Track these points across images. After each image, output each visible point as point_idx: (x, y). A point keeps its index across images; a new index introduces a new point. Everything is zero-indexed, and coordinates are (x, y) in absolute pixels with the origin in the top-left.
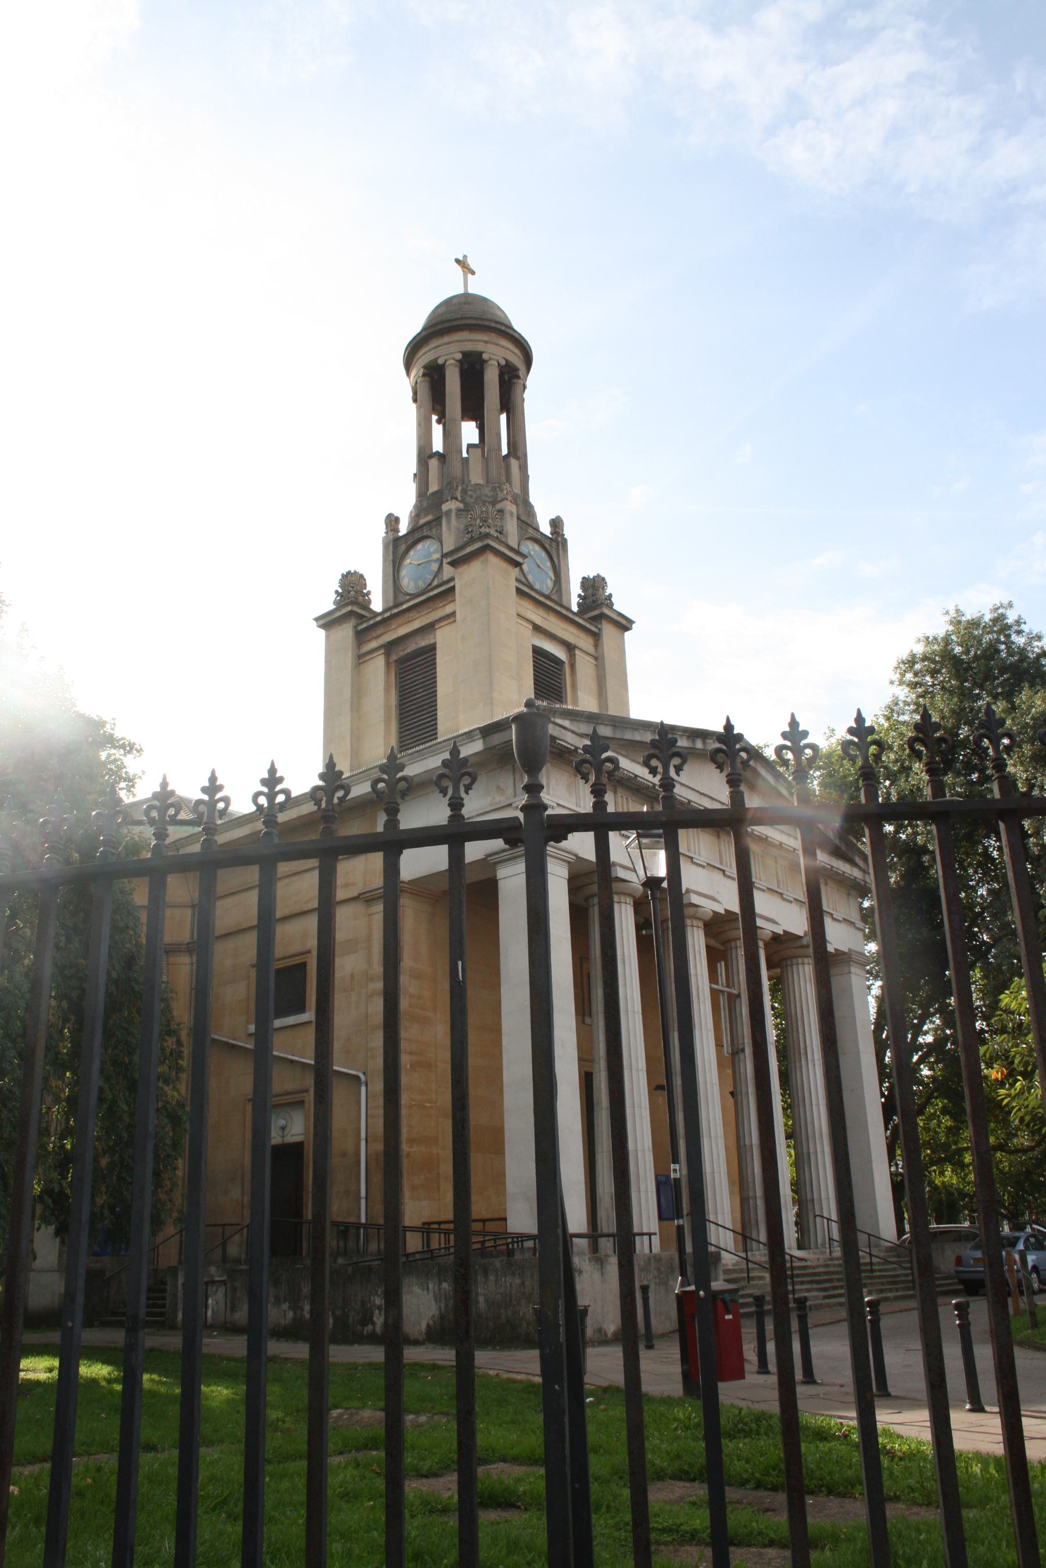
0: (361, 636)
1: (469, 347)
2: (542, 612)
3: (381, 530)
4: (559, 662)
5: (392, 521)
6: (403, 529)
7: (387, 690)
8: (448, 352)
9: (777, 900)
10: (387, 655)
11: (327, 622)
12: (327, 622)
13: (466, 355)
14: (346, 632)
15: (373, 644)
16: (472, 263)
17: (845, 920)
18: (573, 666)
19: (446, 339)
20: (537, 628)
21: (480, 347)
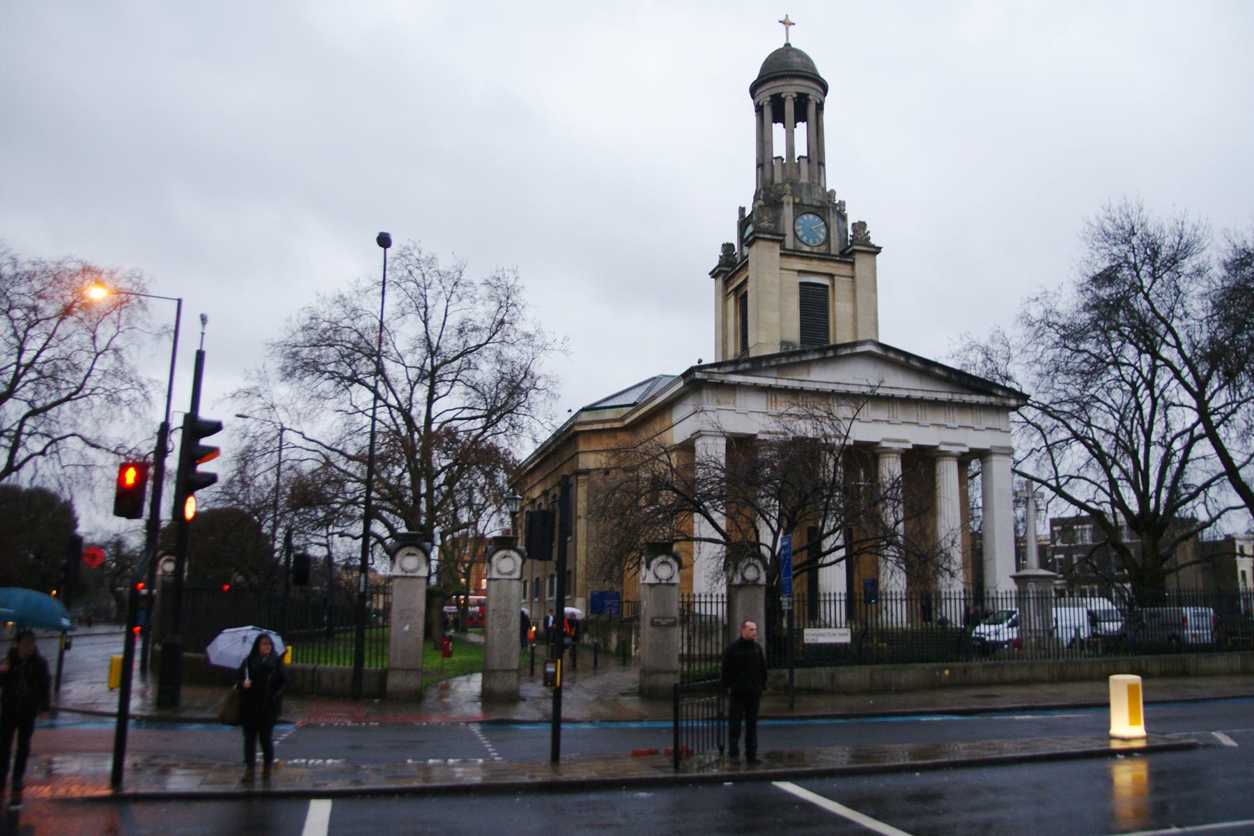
0: (726, 283)
1: (774, 91)
2: (806, 262)
3: (736, 217)
4: (826, 287)
5: (742, 210)
6: (747, 213)
7: (736, 315)
8: (765, 96)
9: (914, 428)
10: (736, 295)
11: (714, 274)
12: (714, 274)
13: (772, 96)
14: (720, 281)
15: (730, 289)
16: (791, 19)
17: (988, 429)
18: (833, 286)
19: (764, 88)
20: (800, 272)
21: (780, 90)
